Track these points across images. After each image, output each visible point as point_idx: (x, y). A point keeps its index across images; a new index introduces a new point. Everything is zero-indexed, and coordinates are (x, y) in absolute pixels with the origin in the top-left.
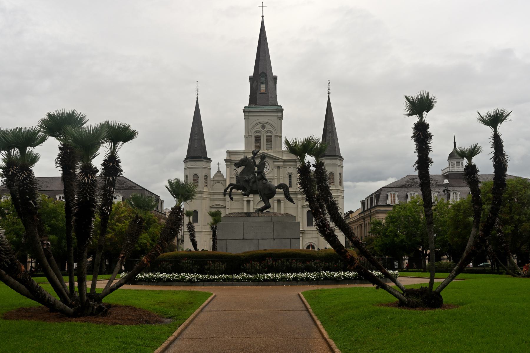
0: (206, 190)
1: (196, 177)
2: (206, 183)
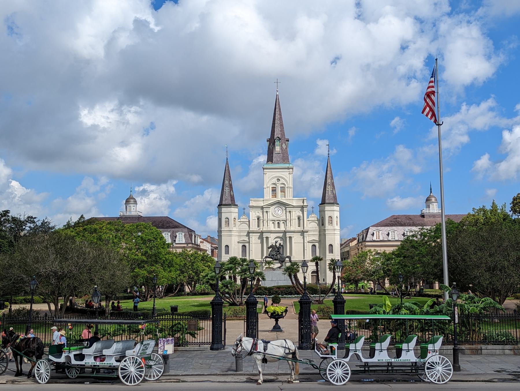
0: (234, 229)
1: (227, 220)
2: (235, 224)
